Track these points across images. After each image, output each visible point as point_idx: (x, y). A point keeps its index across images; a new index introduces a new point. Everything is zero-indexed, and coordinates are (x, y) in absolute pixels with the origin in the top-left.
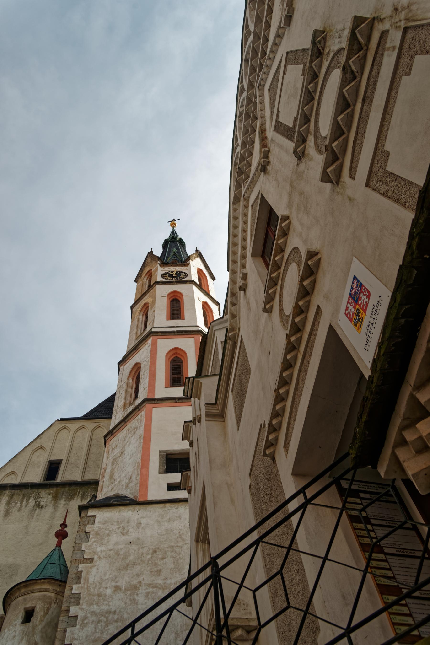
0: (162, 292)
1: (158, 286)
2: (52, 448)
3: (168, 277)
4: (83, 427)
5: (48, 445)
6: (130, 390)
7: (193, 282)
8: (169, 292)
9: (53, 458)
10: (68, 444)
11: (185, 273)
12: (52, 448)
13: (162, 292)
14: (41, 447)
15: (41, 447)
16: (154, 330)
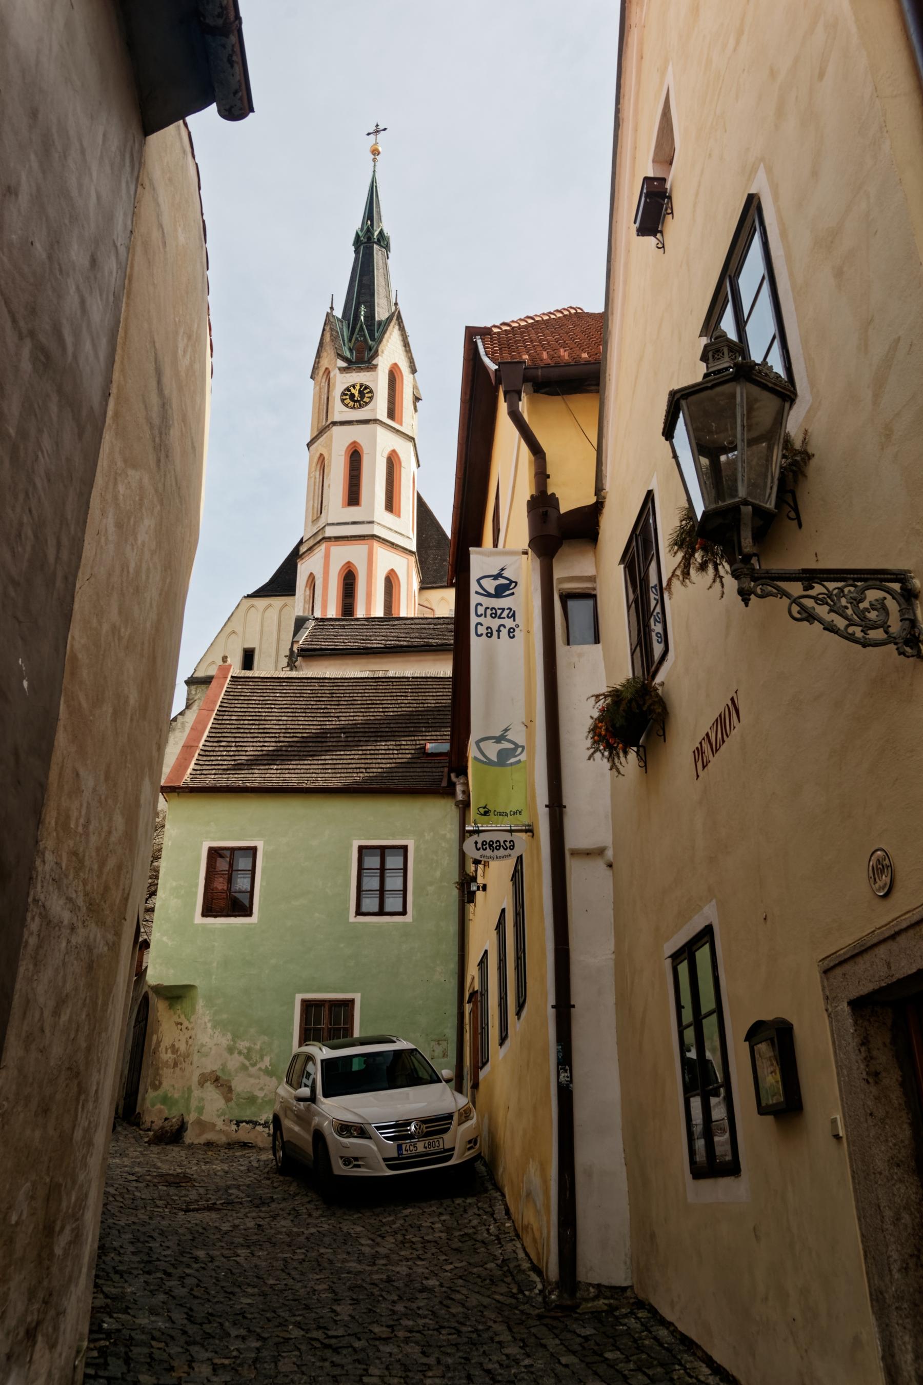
0: (341, 439)
1: (335, 429)
2: (244, 632)
3: (348, 401)
4: (270, 605)
5: (239, 629)
6: (307, 606)
7: (376, 421)
8: (347, 444)
9: (247, 646)
10: (258, 628)
11: (371, 392)
12: (244, 632)
13: (341, 439)
14: (234, 632)
15: (234, 632)
16: (330, 532)
